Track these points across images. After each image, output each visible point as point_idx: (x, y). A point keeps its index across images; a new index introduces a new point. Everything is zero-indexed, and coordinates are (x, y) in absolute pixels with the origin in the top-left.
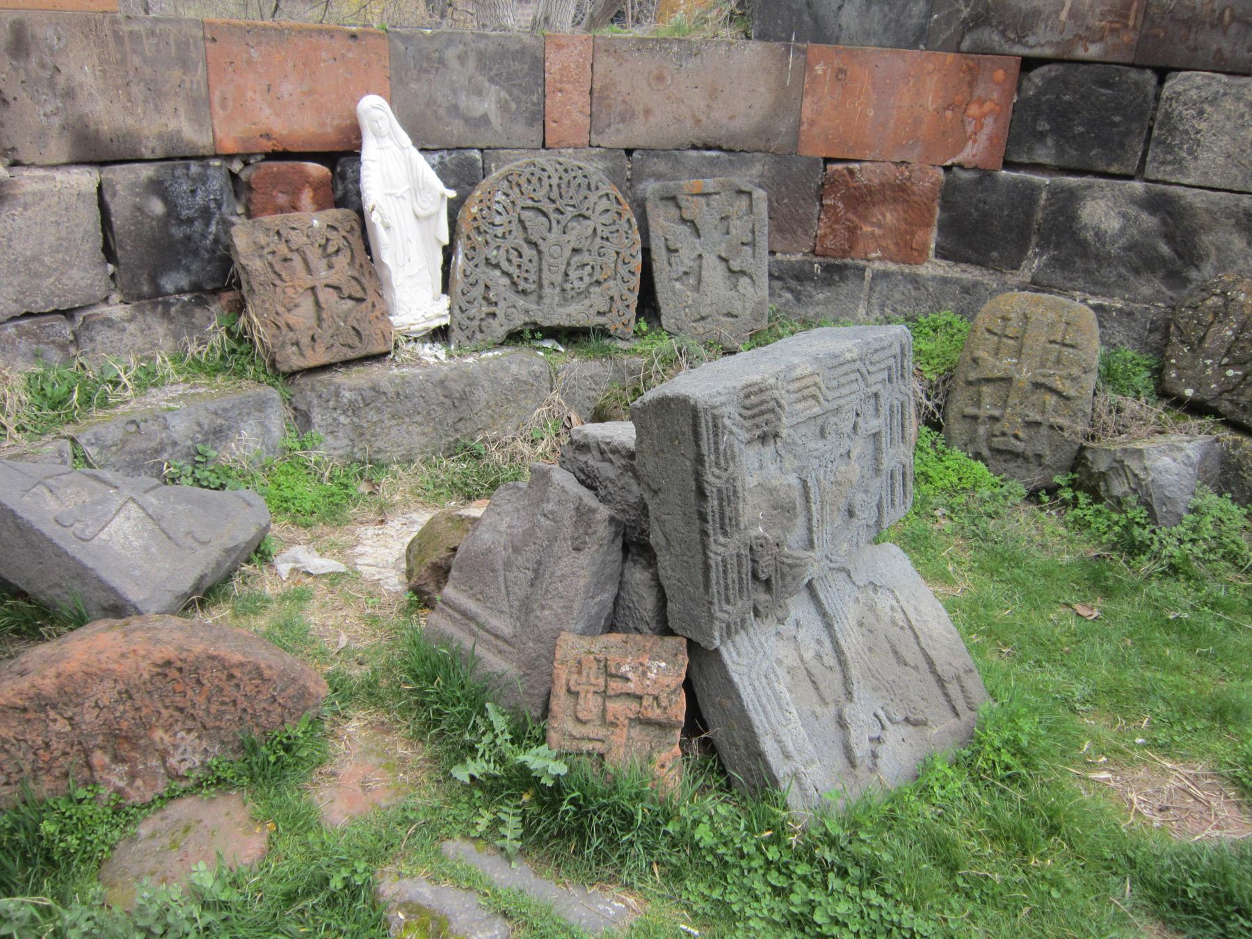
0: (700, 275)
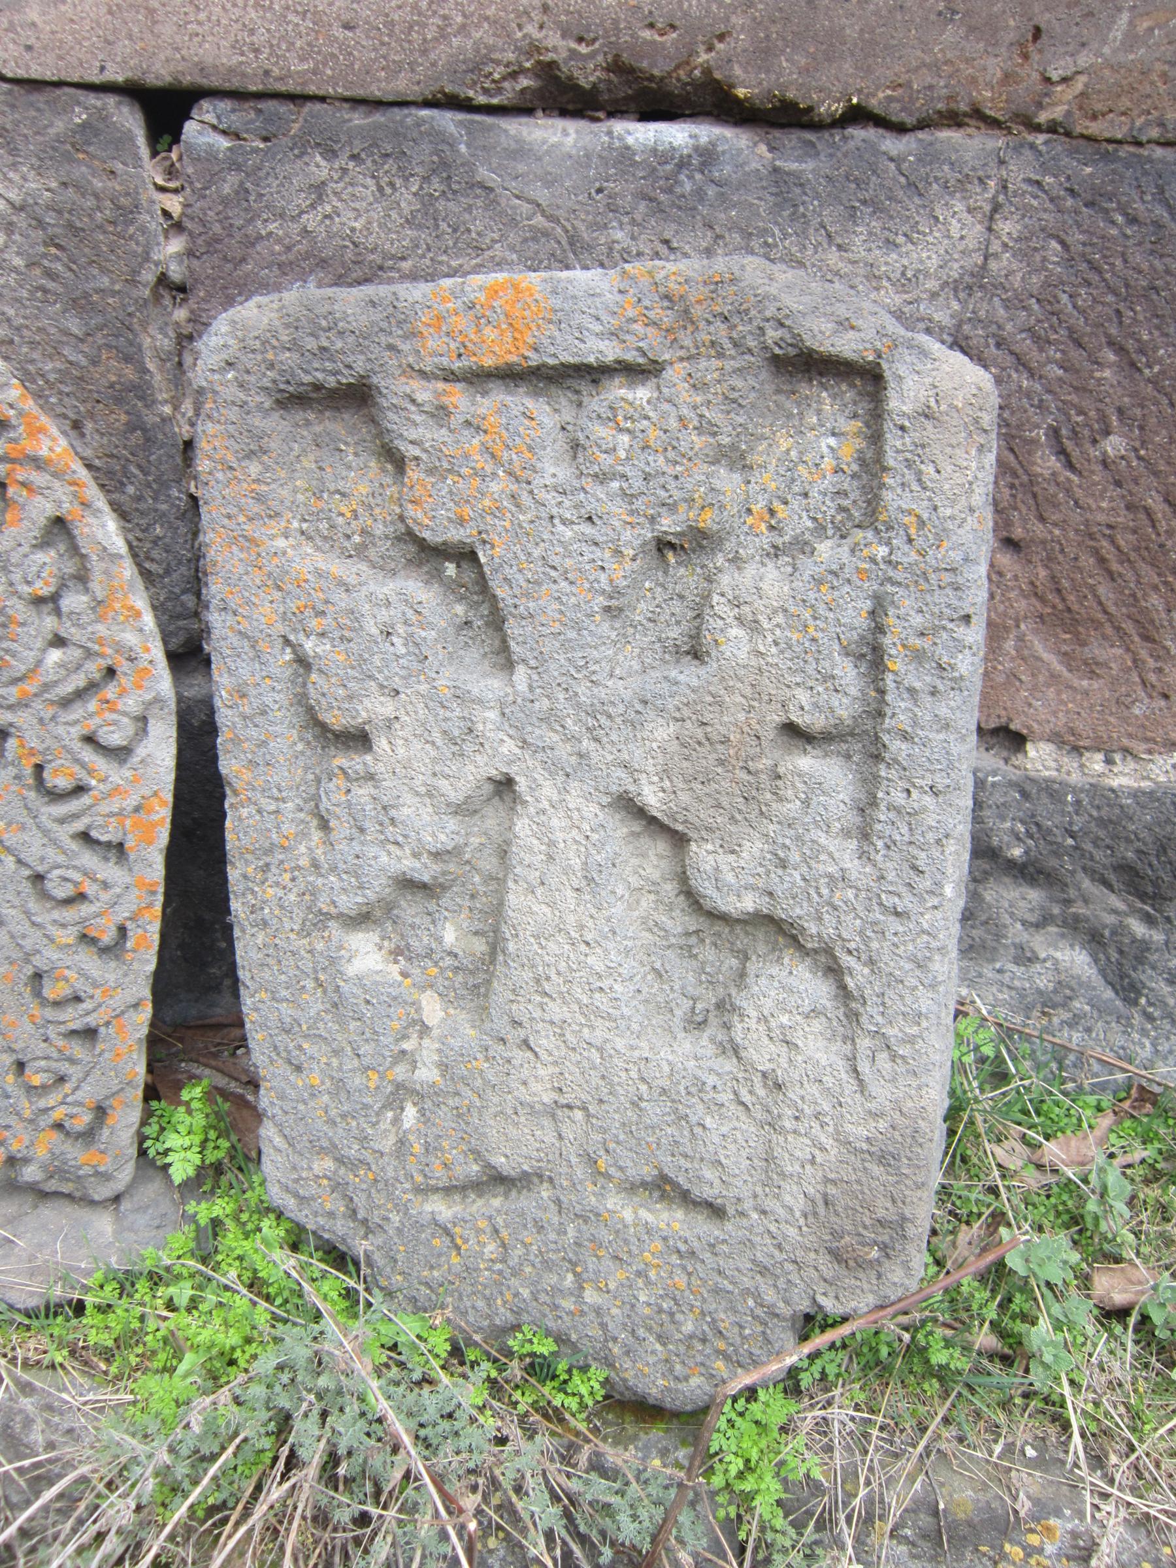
0: (497, 910)
